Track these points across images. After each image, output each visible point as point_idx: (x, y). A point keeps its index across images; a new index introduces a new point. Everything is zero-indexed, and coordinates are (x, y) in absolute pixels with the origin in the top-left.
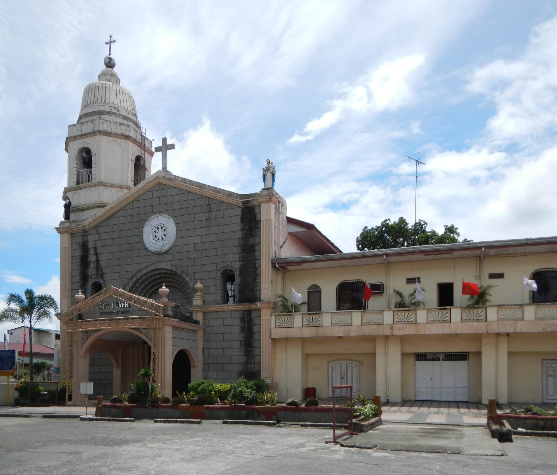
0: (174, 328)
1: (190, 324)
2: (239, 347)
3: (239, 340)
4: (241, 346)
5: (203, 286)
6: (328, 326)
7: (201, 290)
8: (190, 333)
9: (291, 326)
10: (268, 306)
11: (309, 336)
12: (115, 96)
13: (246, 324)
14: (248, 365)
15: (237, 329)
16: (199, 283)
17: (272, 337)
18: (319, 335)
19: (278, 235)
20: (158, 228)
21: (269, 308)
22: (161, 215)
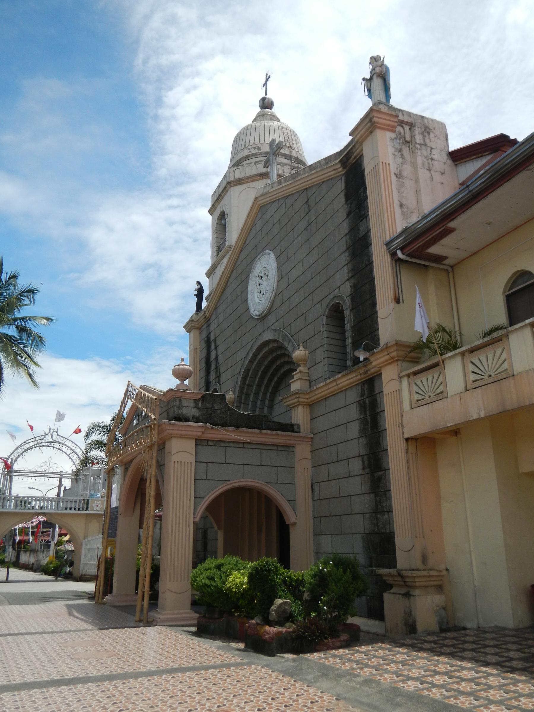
0: (199, 442)
1: (257, 431)
2: (361, 472)
3: (359, 456)
4: (364, 468)
5: (307, 352)
6: (527, 372)
7: (305, 361)
8: (263, 451)
9: (441, 396)
10: (388, 357)
11: (482, 415)
12: (257, 134)
13: (368, 412)
14: (378, 516)
15: (354, 429)
16: (301, 348)
17: (406, 436)
18: (509, 407)
19: (418, 193)
20: (262, 277)
21: (392, 361)
22: (263, 255)
